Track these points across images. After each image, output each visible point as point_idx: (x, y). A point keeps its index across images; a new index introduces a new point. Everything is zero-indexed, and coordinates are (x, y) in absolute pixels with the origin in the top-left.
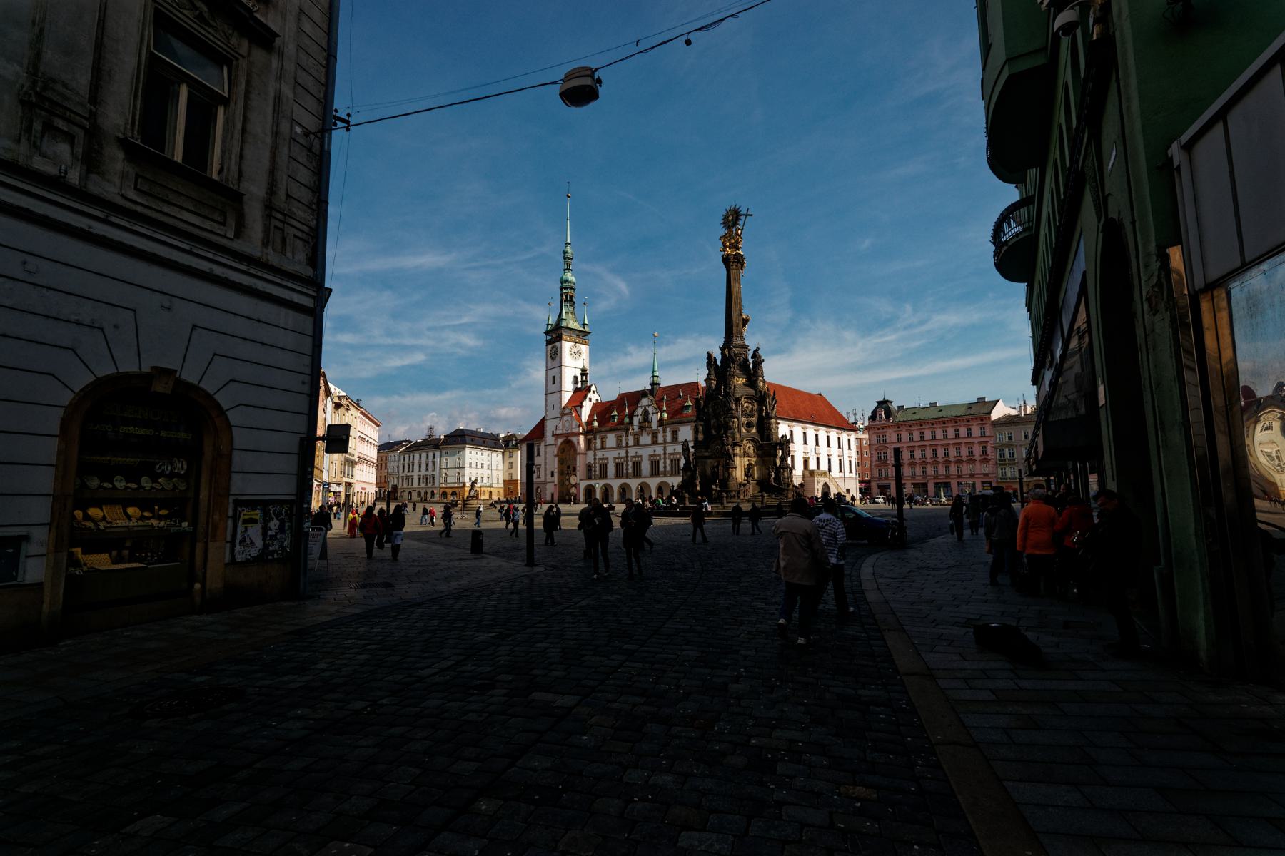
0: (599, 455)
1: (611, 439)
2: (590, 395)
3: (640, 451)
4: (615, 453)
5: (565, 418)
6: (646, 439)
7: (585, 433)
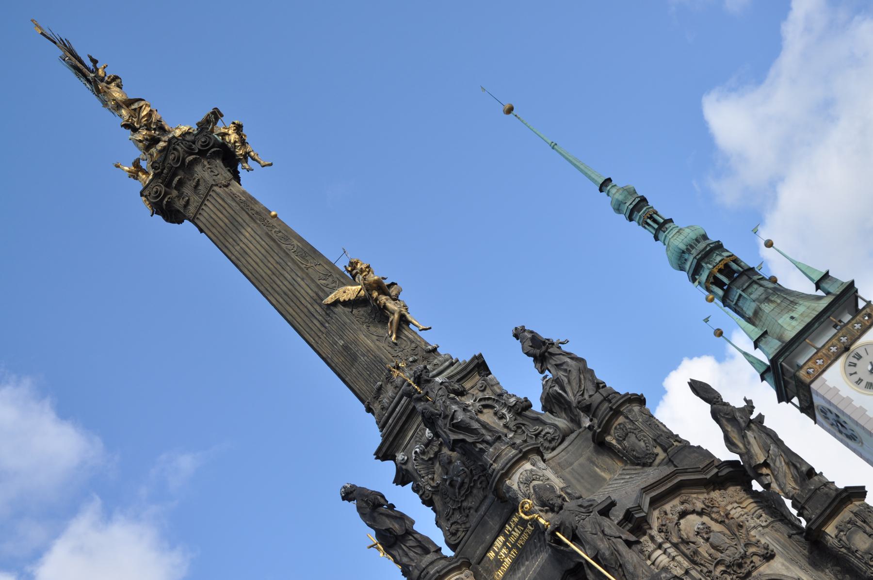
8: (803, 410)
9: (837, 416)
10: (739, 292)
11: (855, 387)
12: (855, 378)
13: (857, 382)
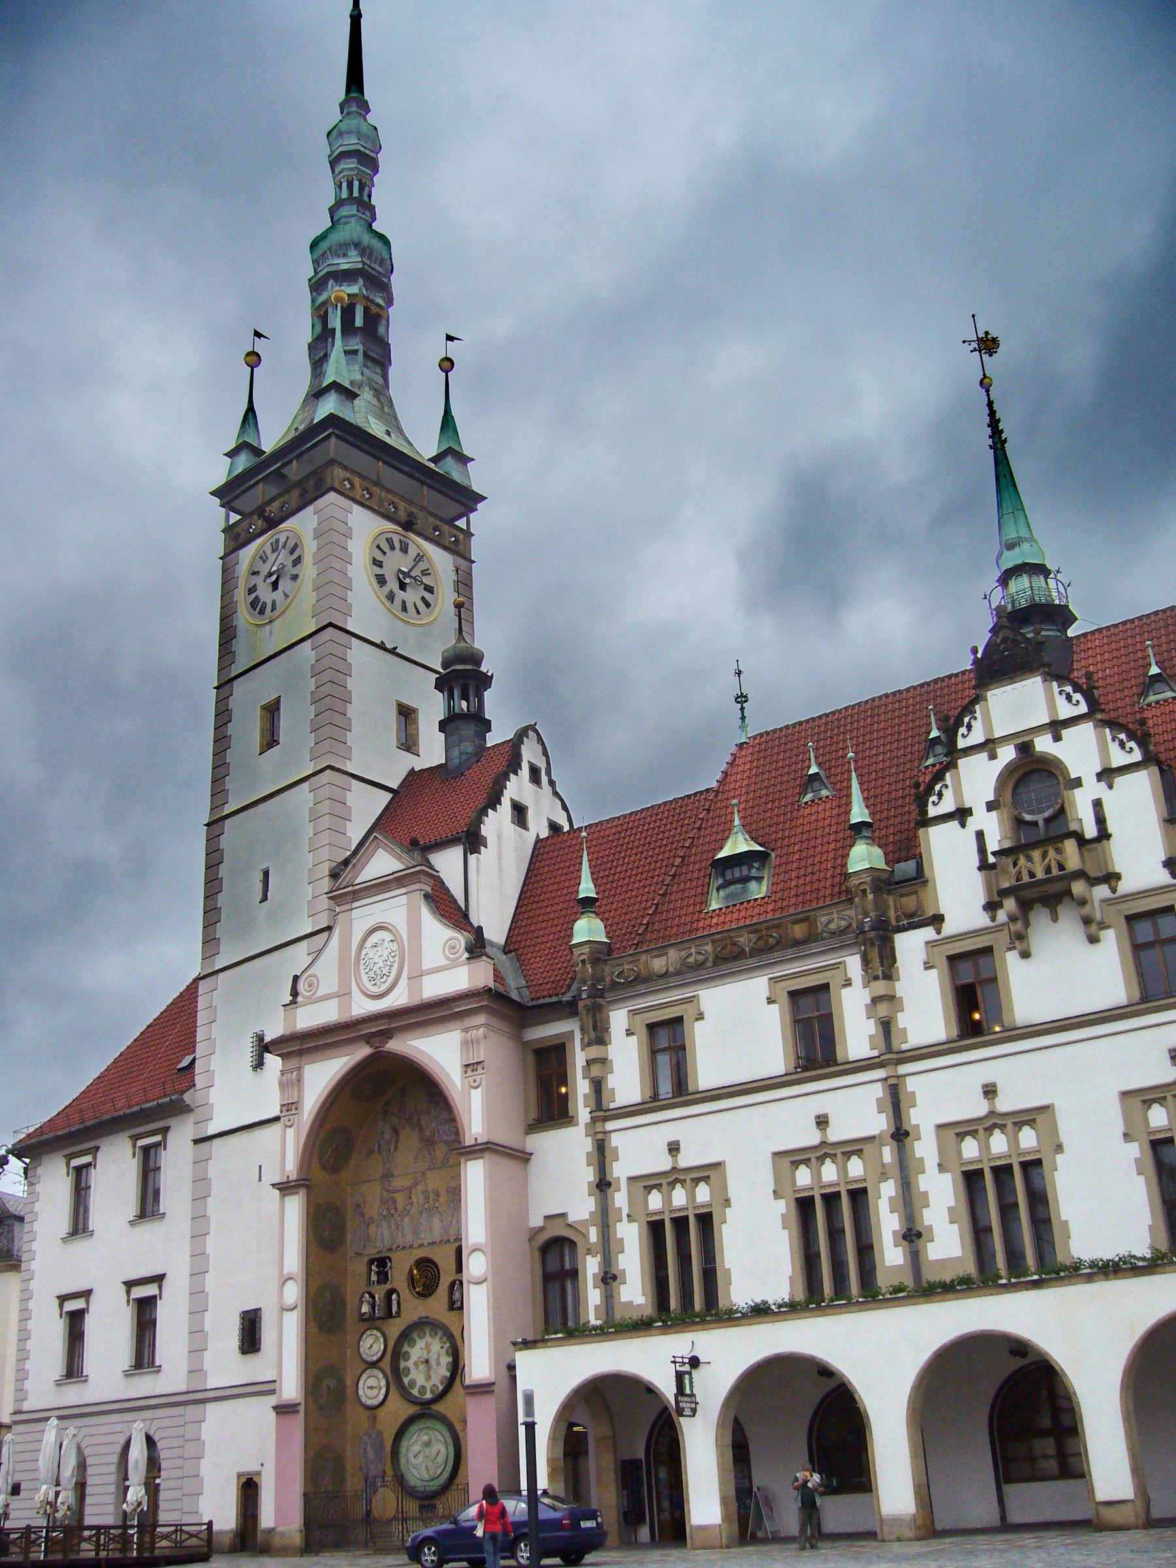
0: (639, 1149)
1: (737, 1023)
2: (517, 787)
3: (1020, 1076)
4: (790, 1120)
5: (364, 916)
6: (1066, 970)
7: (504, 1007)
8: (228, 530)
9: (297, 562)
10: (361, 348)
11: (368, 562)
12: (379, 556)
13: (374, 559)
